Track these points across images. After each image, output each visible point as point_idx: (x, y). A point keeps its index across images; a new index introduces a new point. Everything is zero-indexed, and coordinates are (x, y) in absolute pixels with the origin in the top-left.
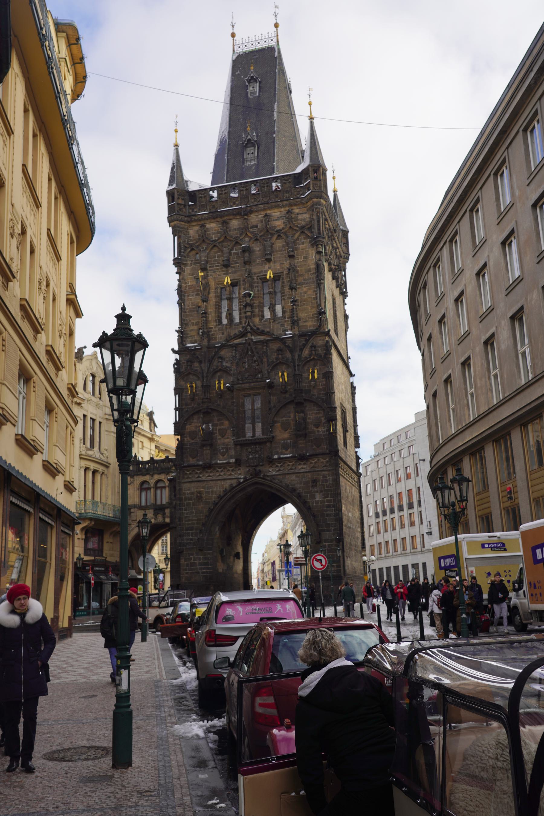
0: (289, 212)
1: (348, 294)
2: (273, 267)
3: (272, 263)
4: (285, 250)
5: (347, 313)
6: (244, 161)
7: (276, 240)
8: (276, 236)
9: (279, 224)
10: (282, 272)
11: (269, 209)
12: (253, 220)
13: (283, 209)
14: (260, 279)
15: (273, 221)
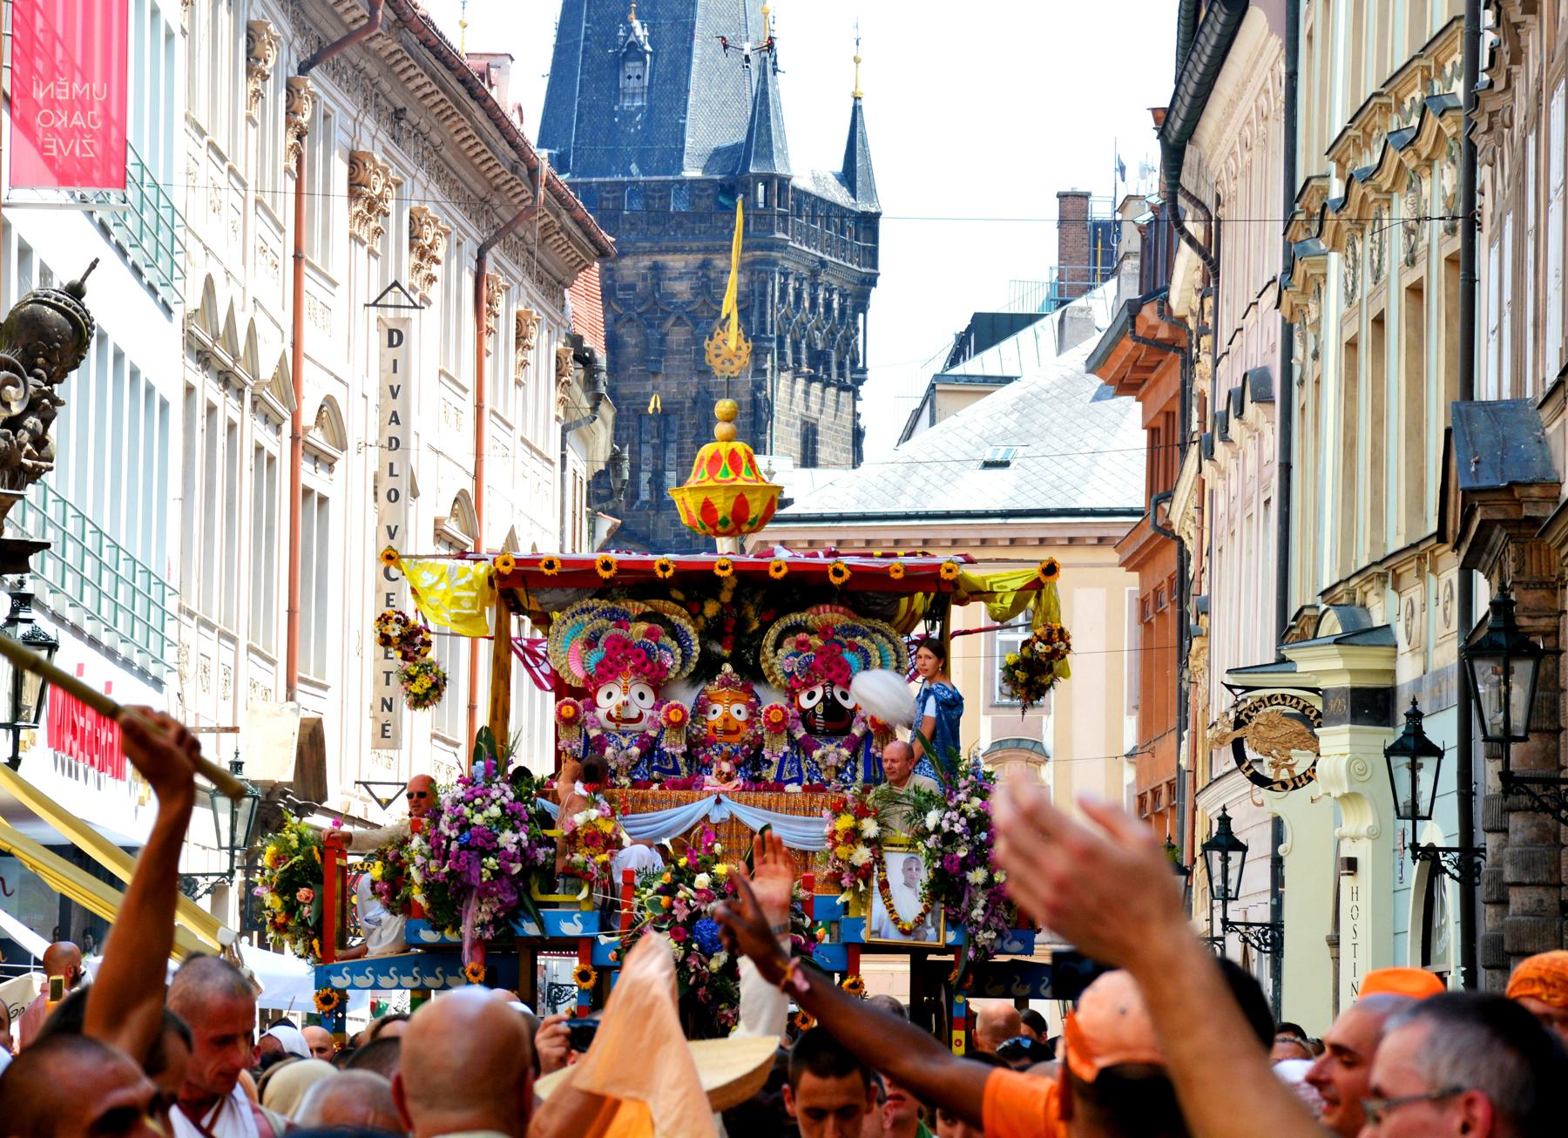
0: (705, 265)
1: (869, 374)
2: (662, 387)
3: (660, 379)
4: (690, 352)
5: (862, 422)
6: (617, 93)
7: (673, 325)
8: (672, 320)
9: (682, 289)
10: (682, 403)
11: (660, 252)
12: (625, 272)
13: (691, 257)
14: (635, 411)
15: (670, 279)
